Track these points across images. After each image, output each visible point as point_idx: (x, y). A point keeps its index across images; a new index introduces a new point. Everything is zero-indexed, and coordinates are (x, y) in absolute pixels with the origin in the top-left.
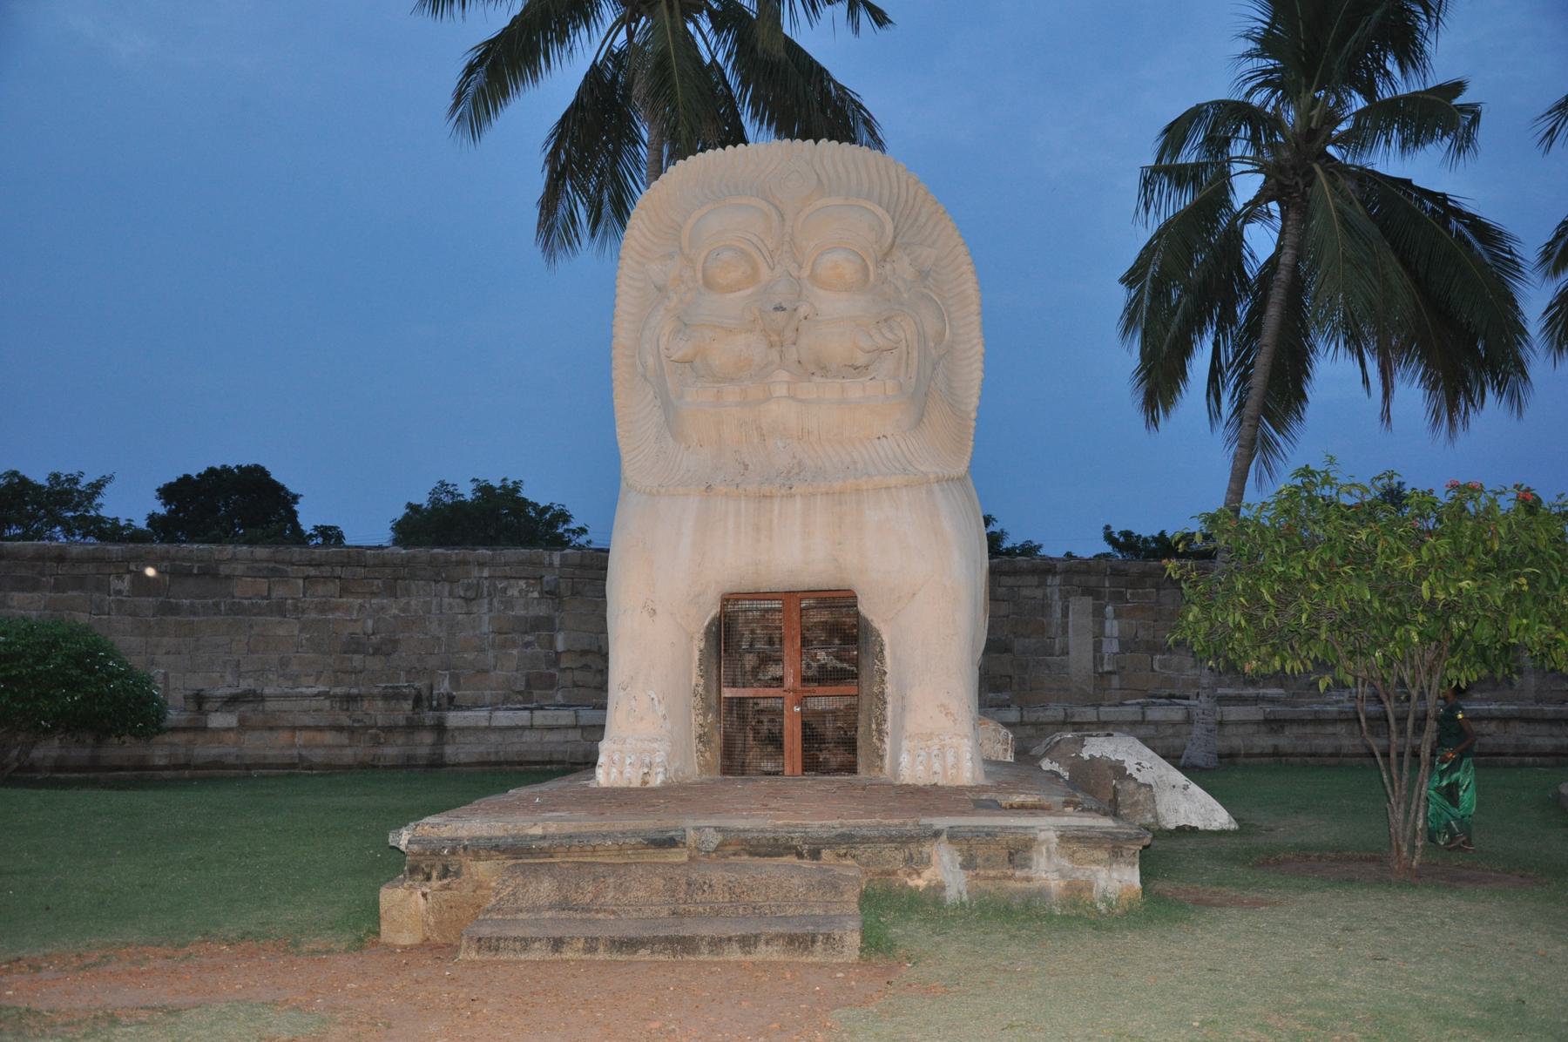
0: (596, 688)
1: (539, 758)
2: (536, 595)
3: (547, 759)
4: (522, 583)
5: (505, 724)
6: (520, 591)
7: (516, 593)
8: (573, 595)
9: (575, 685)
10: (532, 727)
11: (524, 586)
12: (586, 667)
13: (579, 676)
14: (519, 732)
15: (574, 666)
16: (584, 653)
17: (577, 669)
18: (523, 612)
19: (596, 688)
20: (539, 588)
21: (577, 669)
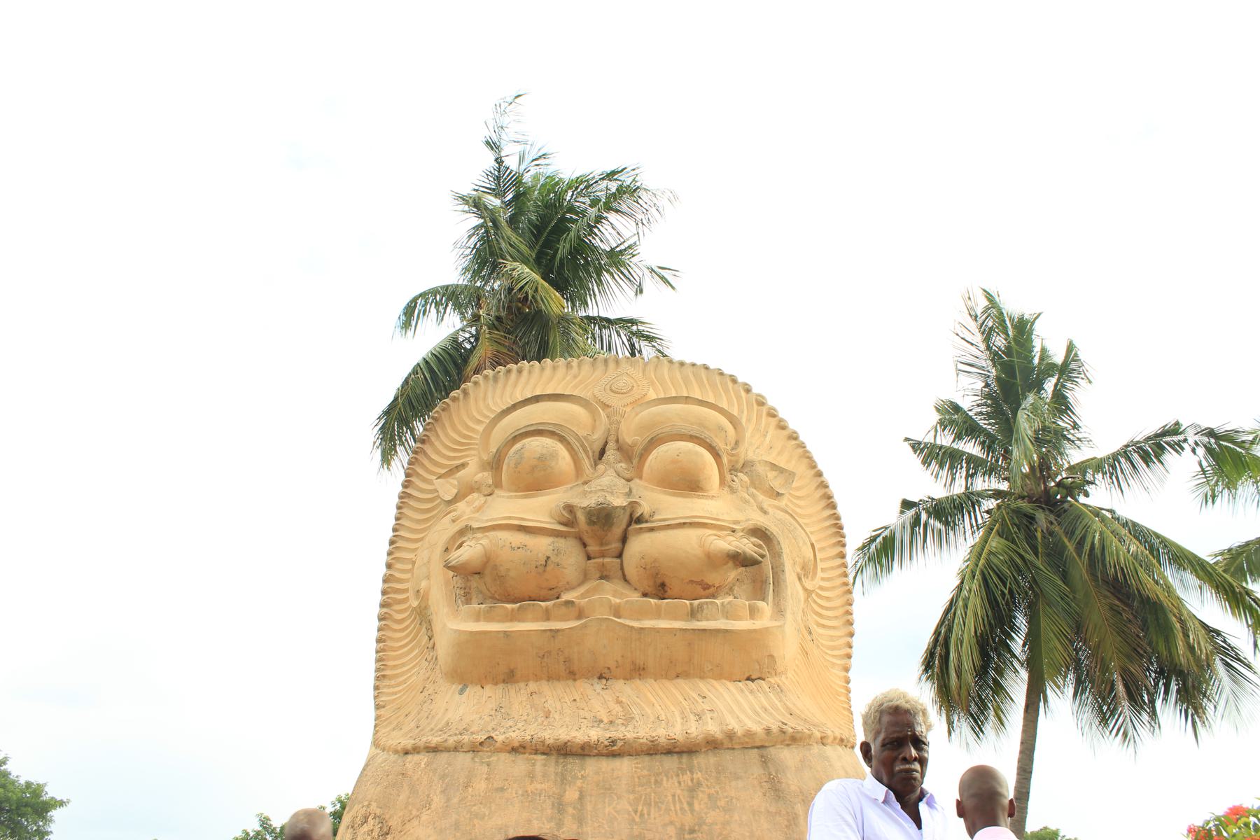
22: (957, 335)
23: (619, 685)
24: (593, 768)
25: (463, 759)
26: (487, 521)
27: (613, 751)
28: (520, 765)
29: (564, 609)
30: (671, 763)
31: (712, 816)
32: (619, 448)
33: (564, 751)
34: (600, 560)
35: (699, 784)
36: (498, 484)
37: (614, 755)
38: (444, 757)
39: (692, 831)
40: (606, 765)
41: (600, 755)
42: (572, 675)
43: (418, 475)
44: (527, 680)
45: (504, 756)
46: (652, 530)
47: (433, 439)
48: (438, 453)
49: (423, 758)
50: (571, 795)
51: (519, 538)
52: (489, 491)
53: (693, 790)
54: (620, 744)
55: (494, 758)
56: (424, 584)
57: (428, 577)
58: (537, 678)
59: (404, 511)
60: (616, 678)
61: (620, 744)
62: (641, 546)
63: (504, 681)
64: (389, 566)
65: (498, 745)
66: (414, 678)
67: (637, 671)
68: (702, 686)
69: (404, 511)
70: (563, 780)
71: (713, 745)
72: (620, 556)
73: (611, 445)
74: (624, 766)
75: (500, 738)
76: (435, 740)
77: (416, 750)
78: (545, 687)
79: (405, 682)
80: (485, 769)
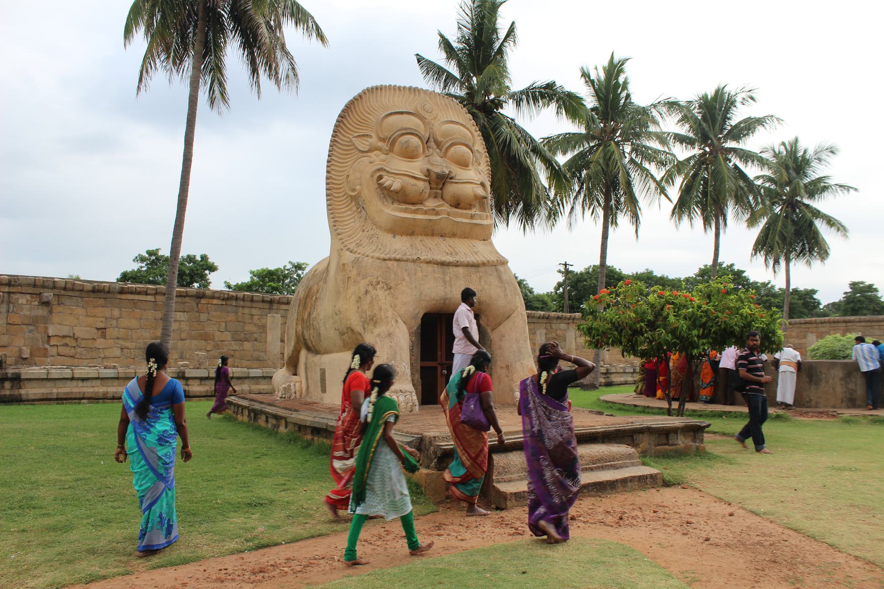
0: (71, 357)
1: (78, 396)
2: (36, 303)
3: (82, 396)
4: (28, 297)
5: (57, 377)
6: (27, 301)
7: (25, 302)
8: (58, 304)
9: (59, 355)
10: (73, 379)
11: (29, 298)
12: (66, 345)
13: (62, 350)
14: (64, 381)
15: (58, 344)
16: (64, 337)
17: (60, 345)
18: (28, 313)
19: (71, 357)
20: (38, 300)
21: (60, 345)
22: (461, 7)
23: (448, 239)
24: (452, 269)
25: (411, 265)
26: (395, 170)
27: (457, 265)
28: (430, 268)
29: (431, 212)
30: (473, 269)
31: (486, 287)
32: (435, 142)
33: (443, 264)
34: (435, 191)
35: (482, 277)
36: (391, 150)
37: (457, 266)
38: (403, 263)
39: (481, 291)
40: (455, 269)
41: (453, 266)
42: (433, 235)
43: (340, 132)
44: (417, 235)
45: (425, 265)
46: (456, 183)
47: (347, 117)
48: (350, 124)
49: (395, 263)
50: (447, 279)
51: (413, 181)
52: (387, 153)
53: (480, 278)
54: (459, 262)
55: (421, 265)
56: (358, 187)
57: (361, 185)
58: (421, 235)
59: (334, 148)
60: (447, 237)
61: (459, 262)
62: (451, 189)
63: (410, 235)
64: (328, 172)
65: (422, 260)
66: (353, 224)
67: (454, 235)
68: (472, 241)
69: (334, 148)
70: (444, 274)
71: (484, 264)
72: (441, 189)
73: (432, 139)
74: (461, 270)
75: (422, 258)
76: (398, 257)
77: (390, 259)
78: (424, 238)
79: (348, 225)
80: (419, 269)
